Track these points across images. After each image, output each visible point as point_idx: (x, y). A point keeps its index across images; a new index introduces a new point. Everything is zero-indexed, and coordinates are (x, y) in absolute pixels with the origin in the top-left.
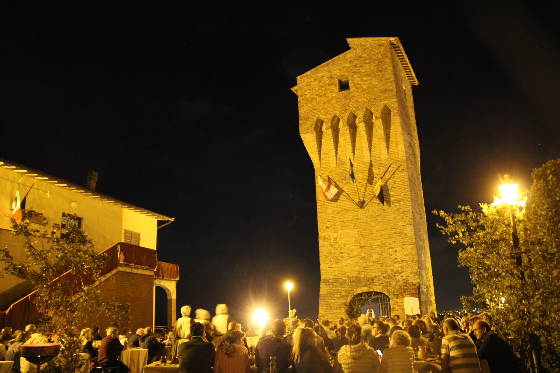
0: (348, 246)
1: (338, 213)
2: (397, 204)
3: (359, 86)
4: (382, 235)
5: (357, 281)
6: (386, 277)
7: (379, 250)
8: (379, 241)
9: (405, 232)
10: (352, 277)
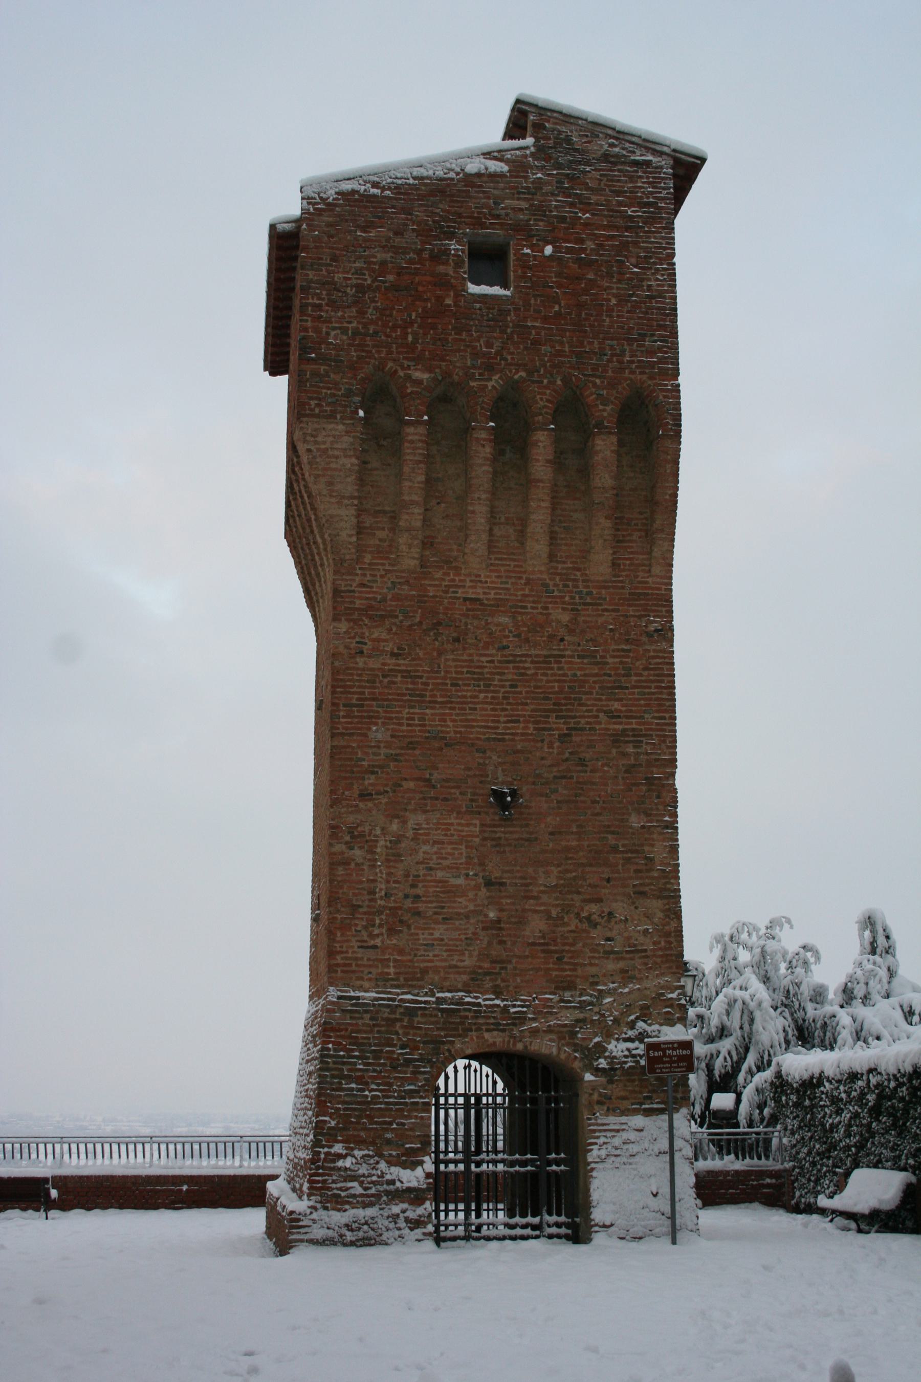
0: (440, 874)
1: (412, 745)
2: (630, 749)
8: (555, 870)
9: (646, 848)
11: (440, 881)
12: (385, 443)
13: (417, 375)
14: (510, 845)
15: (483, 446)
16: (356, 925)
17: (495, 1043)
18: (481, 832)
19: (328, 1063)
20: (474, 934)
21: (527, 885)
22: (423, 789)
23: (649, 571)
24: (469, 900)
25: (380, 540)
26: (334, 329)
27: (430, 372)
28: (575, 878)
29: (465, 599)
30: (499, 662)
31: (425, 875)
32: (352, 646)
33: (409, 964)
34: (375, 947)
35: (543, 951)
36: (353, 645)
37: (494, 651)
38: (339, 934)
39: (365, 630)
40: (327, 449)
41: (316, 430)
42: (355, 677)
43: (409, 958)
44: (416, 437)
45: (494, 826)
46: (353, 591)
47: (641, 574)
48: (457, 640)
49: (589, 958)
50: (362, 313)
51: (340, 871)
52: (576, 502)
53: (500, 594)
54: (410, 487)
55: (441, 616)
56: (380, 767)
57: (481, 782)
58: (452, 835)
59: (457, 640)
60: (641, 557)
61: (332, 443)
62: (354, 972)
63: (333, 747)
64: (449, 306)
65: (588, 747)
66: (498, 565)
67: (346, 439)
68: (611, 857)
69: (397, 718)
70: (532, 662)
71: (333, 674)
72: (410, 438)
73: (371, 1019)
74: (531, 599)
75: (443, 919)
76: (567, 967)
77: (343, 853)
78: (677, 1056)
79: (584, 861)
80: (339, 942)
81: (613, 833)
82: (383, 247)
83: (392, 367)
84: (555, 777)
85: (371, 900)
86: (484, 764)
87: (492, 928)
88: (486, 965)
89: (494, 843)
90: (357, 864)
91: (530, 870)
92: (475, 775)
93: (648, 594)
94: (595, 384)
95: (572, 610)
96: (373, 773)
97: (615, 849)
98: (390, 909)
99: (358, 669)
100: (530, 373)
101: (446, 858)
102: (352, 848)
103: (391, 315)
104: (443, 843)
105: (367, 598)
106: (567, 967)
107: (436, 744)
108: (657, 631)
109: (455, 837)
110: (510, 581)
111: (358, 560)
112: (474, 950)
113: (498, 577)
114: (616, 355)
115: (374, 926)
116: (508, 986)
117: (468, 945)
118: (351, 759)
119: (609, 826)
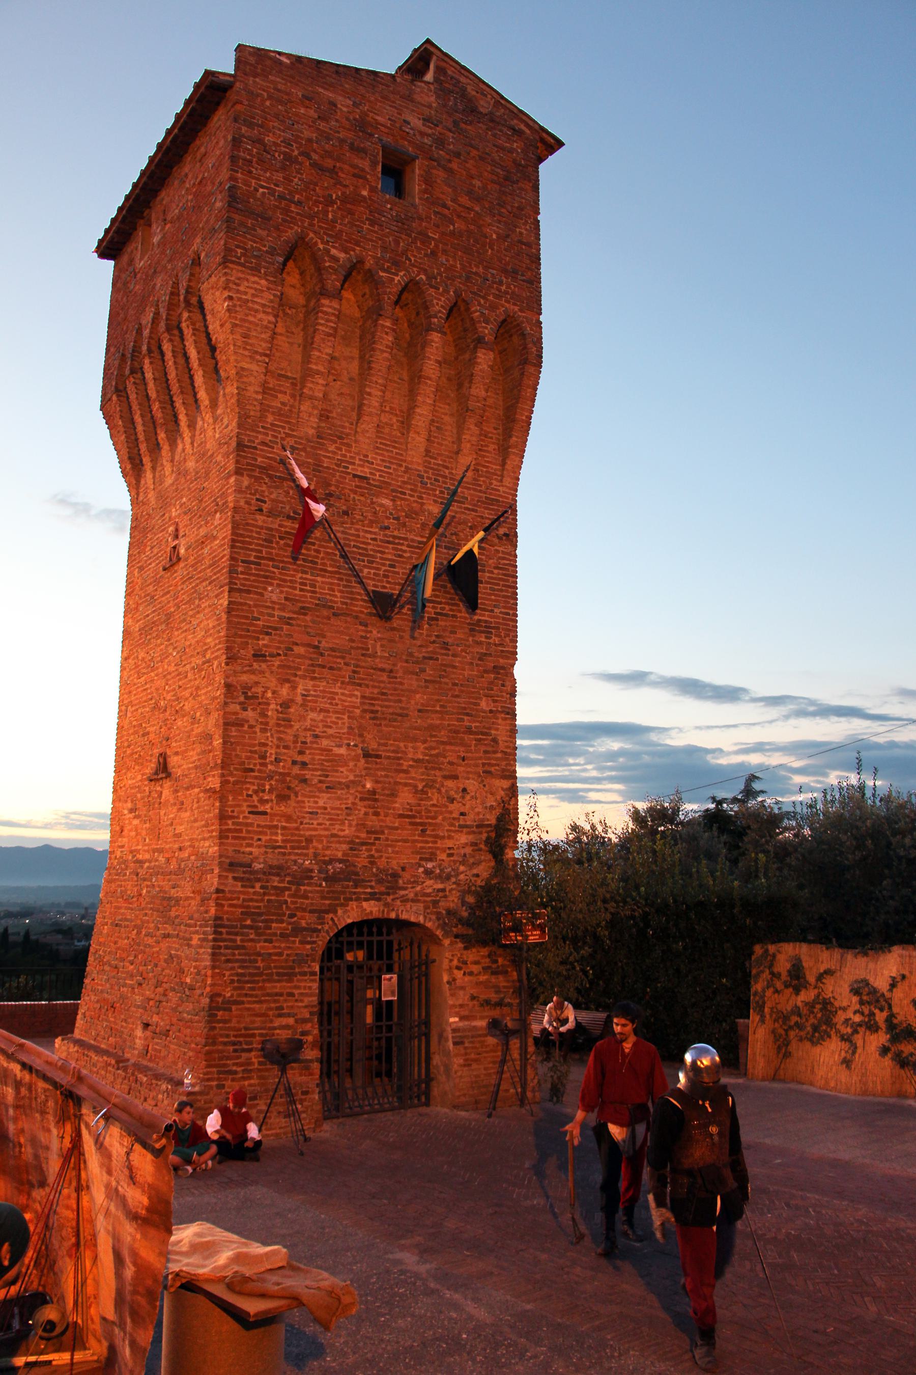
0: (325, 743)
1: (303, 611)
3: (446, 212)
4: (431, 727)
5: (343, 879)
7: (417, 774)
8: (422, 746)
9: (493, 732)
10: (331, 861)
11: (325, 750)
12: (289, 312)
13: (334, 252)
14: (385, 719)
15: (387, 334)
16: (248, 789)
17: (371, 912)
18: (362, 703)
19: (221, 933)
20: (354, 804)
21: (399, 759)
22: (313, 656)
23: (501, 481)
24: (351, 771)
25: (283, 403)
26: (262, 187)
27: (346, 253)
28: (437, 755)
29: (355, 476)
30: (381, 541)
31: (312, 742)
32: (253, 502)
33: (297, 832)
34: (265, 813)
35: (412, 824)
36: (253, 502)
37: (377, 530)
38: (230, 798)
39: (264, 488)
40: (248, 301)
41: (239, 279)
42: (254, 535)
43: (295, 825)
44: (330, 310)
45: (372, 699)
46: (255, 448)
47: (495, 482)
48: (346, 513)
49: (447, 831)
50: (288, 179)
51: (234, 732)
52: (447, 407)
53: (384, 477)
54: (319, 357)
55: (333, 488)
56: (275, 629)
57: (363, 655)
58: (337, 705)
59: (346, 513)
60: (494, 467)
61: (253, 295)
62: (244, 838)
63: (230, 603)
64: (364, 197)
65: (451, 632)
66: (383, 450)
67: (266, 295)
68: (466, 737)
69: (291, 581)
70: (408, 546)
71: (233, 528)
72: (325, 309)
73: (262, 887)
74: (409, 487)
75: (327, 787)
76: (430, 839)
77: (236, 713)
79: (445, 740)
80: (231, 806)
81: (467, 715)
82: (310, 126)
83: (312, 238)
84: (424, 658)
85: (262, 764)
86: (366, 638)
87: (369, 799)
88: (363, 835)
89: (372, 715)
90: (251, 727)
91: (402, 745)
92: (358, 648)
93: (498, 501)
94: (479, 304)
95: (442, 503)
96: (267, 634)
97: (469, 731)
98: (281, 774)
99: (257, 526)
100: (429, 278)
101: (330, 727)
102: (245, 709)
103: (314, 190)
104: (328, 711)
105: (268, 458)
106: (430, 839)
107: (325, 613)
108: (505, 535)
109: (340, 707)
110: (393, 466)
111: (262, 418)
112: (353, 820)
113: (383, 461)
114: (495, 283)
115: (264, 791)
116: (381, 856)
117: (348, 815)
118: (247, 618)
119: (465, 708)
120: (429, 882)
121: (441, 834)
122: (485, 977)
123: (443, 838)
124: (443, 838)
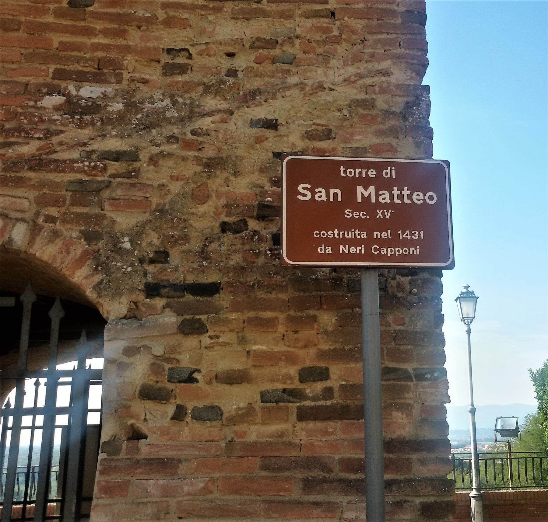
6: (93, 107)
76: (99, 26)
78: (391, 205)
120: (73, 133)
121: (141, 13)
122: (274, 428)
123: (151, 21)
124: (151, 21)
